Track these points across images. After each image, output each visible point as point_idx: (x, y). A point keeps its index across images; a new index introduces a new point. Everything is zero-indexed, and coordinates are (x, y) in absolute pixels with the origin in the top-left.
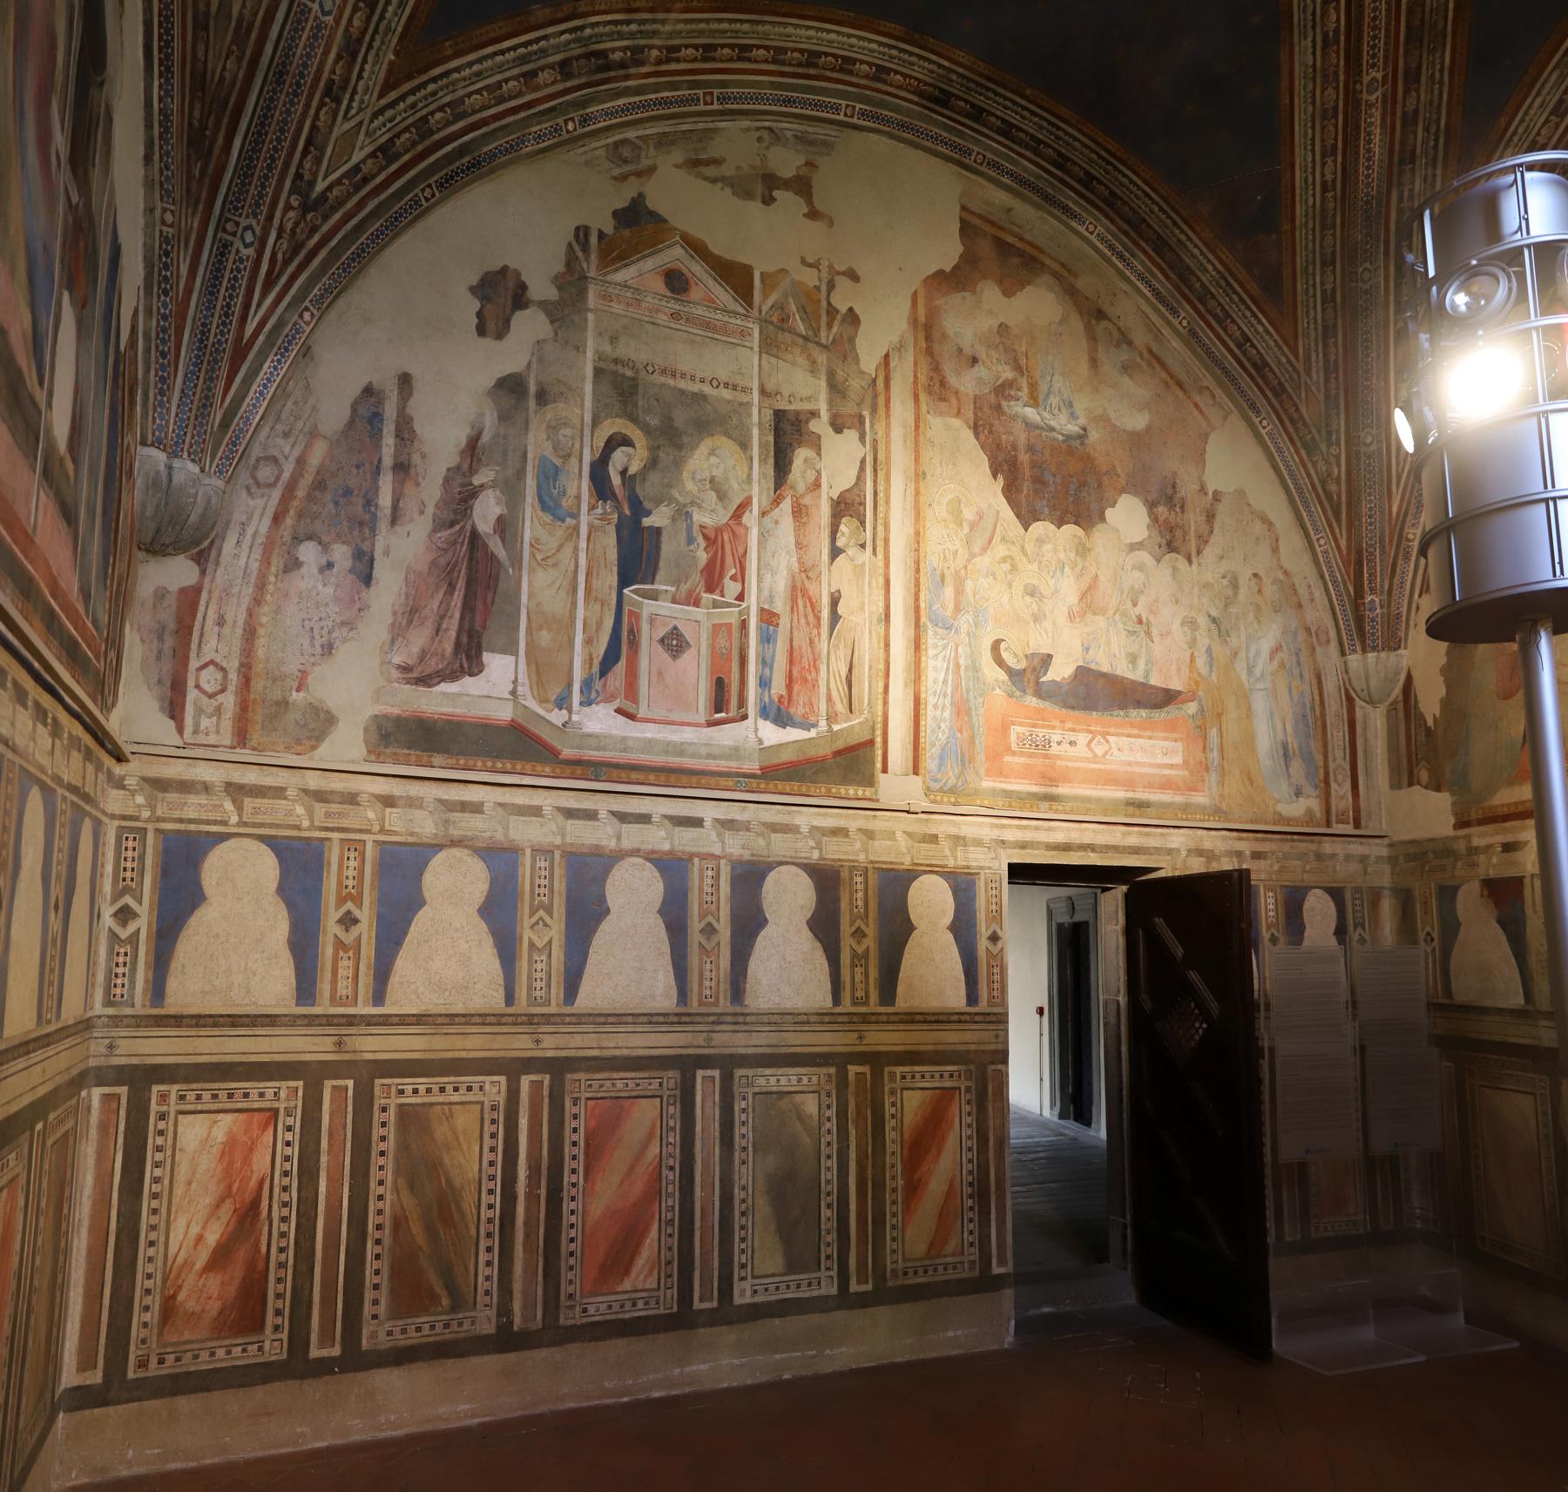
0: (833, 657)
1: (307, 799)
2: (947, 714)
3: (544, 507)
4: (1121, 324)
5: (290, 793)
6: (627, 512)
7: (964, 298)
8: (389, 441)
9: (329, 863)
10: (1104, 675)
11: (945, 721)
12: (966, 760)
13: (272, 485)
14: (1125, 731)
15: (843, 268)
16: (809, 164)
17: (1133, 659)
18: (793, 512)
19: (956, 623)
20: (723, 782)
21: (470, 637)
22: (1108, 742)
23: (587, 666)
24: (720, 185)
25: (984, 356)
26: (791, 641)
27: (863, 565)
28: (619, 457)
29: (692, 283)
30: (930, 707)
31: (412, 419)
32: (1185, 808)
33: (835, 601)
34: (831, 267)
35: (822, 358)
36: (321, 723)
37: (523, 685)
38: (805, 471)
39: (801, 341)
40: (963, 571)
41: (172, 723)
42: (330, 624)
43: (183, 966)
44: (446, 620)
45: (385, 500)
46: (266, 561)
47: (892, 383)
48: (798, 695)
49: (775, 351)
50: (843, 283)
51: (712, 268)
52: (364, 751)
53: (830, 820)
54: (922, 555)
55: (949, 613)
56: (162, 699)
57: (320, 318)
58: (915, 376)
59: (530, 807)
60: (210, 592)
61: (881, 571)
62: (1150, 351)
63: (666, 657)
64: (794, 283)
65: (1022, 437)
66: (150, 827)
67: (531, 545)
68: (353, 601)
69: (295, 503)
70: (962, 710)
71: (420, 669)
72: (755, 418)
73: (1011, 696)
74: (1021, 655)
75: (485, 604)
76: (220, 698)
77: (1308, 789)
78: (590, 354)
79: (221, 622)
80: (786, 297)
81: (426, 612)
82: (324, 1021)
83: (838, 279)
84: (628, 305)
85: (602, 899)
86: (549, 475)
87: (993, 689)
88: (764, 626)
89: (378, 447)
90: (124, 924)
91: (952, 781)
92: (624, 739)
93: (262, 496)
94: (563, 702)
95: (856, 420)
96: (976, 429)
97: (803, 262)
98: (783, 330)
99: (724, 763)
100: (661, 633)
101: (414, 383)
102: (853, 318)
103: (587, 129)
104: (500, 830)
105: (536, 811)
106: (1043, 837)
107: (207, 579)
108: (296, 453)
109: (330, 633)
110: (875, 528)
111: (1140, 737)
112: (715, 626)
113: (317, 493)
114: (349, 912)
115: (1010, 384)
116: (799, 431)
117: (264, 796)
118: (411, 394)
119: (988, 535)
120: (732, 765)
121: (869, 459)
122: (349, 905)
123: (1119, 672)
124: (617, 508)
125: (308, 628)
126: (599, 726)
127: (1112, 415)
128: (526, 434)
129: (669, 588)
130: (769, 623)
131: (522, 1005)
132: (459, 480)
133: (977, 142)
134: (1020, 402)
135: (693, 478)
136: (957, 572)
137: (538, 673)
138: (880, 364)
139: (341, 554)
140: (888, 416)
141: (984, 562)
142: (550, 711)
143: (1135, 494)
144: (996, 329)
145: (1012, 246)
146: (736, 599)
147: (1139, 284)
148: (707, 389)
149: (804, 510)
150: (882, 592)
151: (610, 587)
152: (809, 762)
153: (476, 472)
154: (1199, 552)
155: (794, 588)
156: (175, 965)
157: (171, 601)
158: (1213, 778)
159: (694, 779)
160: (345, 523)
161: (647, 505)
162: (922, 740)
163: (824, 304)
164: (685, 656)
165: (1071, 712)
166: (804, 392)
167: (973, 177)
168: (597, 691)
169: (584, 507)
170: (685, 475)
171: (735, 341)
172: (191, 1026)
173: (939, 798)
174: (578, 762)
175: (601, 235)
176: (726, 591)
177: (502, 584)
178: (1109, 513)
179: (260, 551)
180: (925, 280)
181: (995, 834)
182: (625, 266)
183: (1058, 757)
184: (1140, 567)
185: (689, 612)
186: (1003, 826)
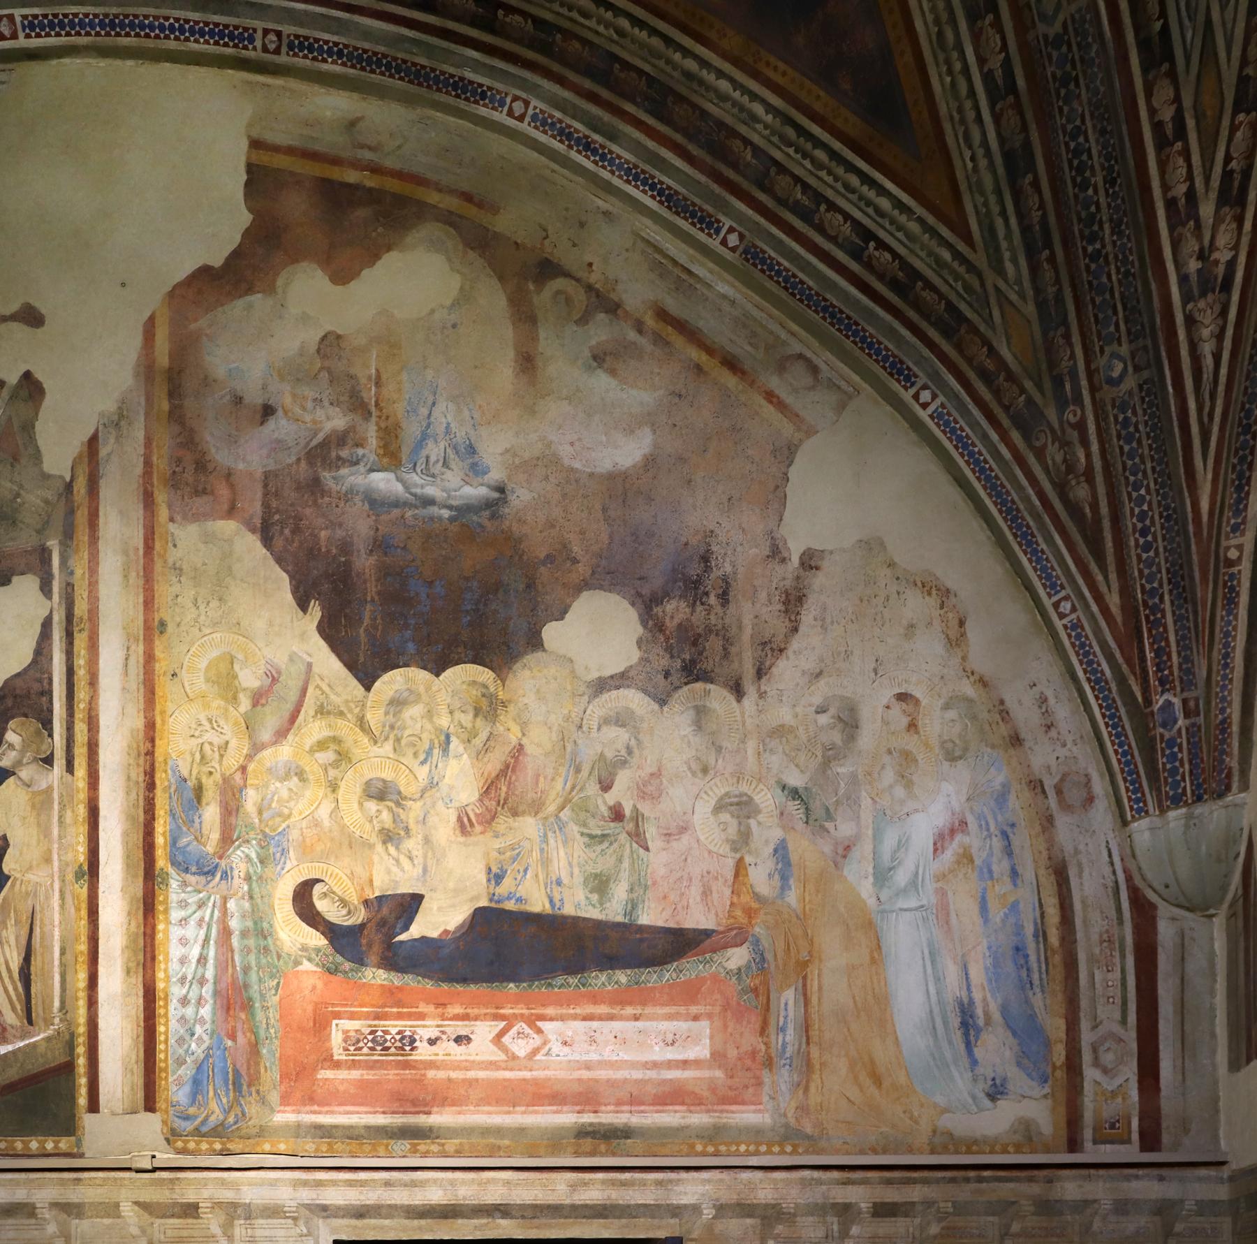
2: (206, 1011)
4: (594, 278)
7: (250, 307)
11: (202, 1021)
14: (578, 1011)
17: (600, 885)
19: (223, 863)
22: (539, 1031)
25: (288, 400)
27: (49, 789)
30: (174, 1004)
32: (714, 1135)
40: (238, 777)
47: (102, 483)
54: (159, 757)
55: (210, 848)
58: (148, 463)
61: (83, 796)
62: (662, 315)
65: (360, 526)
73: (332, 971)
74: (355, 900)
77: (1019, 1081)
87: (297, 963)
91: (216, 1116)
106: (400, 1197)
111: (611, 1018)
115: (341, 439)
119: (289, 707)
123: (569, 910)
127: (565, 451)
134: (361, 468)
136: (226, 780)
138: (80, 456)
140: (94, 539)
141: (284, 752)
144: (313, 348)
147: (630, 189)
150: (83, 829)
154: (760, 673)
158: (784, 1078)
165: (459, 988)
167: (278, 82)
173: (192, 1145)
178: (551, 633)
181: (306, 1195)
183: (432, 1065)
186: (319, 1184)
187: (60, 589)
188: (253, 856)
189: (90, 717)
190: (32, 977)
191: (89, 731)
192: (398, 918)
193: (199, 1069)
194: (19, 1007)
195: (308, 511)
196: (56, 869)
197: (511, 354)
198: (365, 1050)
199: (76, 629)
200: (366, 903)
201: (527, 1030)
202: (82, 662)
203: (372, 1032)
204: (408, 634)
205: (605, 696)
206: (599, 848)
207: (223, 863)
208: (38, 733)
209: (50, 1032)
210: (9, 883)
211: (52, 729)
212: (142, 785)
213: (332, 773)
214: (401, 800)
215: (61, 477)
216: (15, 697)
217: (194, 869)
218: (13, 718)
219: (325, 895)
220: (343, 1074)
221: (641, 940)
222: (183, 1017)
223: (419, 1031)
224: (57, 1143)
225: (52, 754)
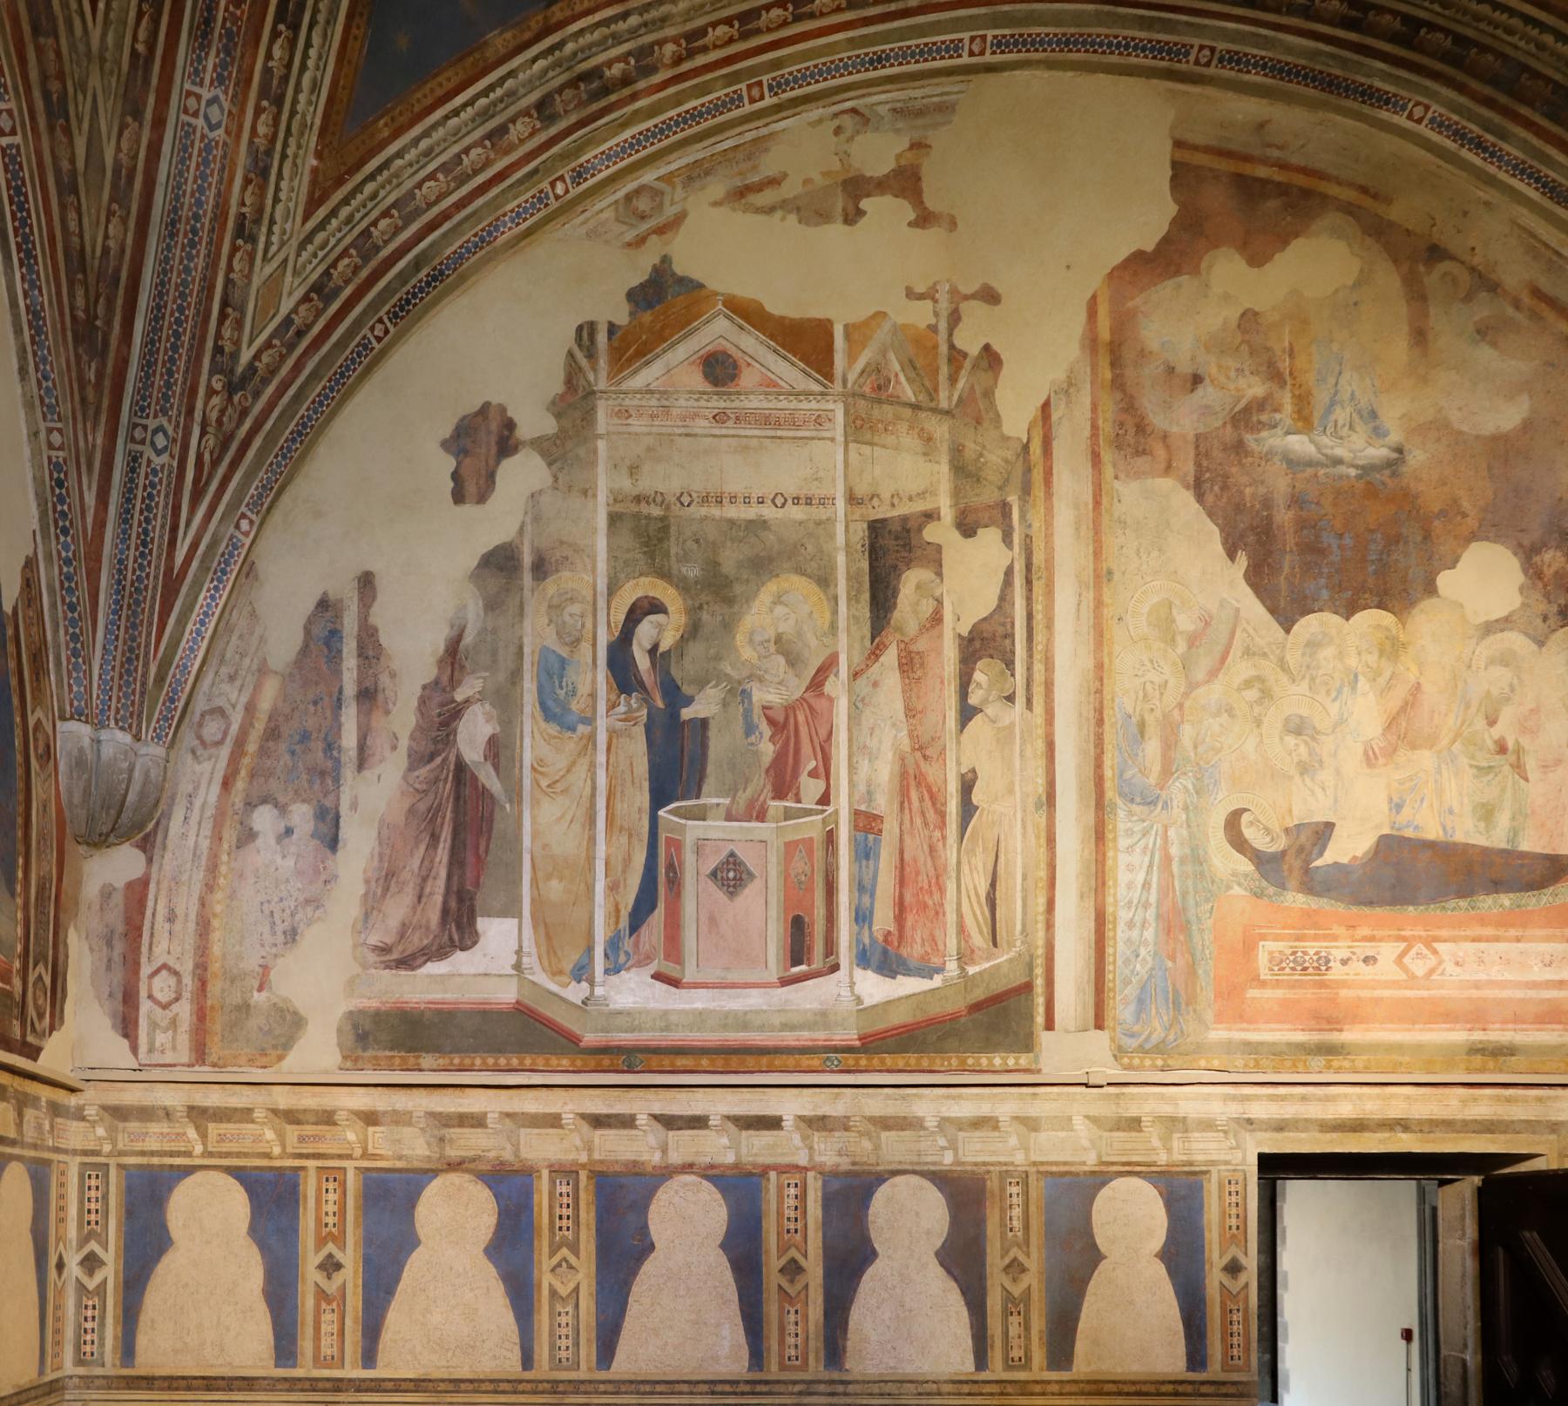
0: (965, 868)
1: (277, 1120)
2: (1149, 934)
3: (548, 715)
5: (259, 1114)
6: (660, 704)
8: (350, 663)
9: (305, 1197)
10: (1431, 845)
11: (1146, 943)
12: (1180, 1001)
13: (220, 743)
14: (1468, 933)
16: (917, 146)
17: (1487, 813)
18: (901, 665)
19: (1164, 794)
20: (806, 1061)
21: (461, 900)
22: (1435, 952)
23: (613, 920)
24: (779, 214)
25: (1214, 370)
26: (902, 852)
27: (1012, 724)
28: (646, 631)
29: (743, 365)
30: (1121, 926)
31: (377, 630)
33: (967, 786)
34: (954, 291)
35: (940, 430)
36: (289, 1025)
37: (529, 955)
38: (917, 604)
39: (908, 412)
40: (1176, 713)
41: (125, 1043)
42: (293, 904)
43: (153, 1321)
44: (430, 882)
45: (349, 739)
46: (218, 838)
47: (1055, 444)
48: (914, 929)
49: (868, 436)
50: (974, 312)
51: (772, 337)
52: (339, 1058)
53: (966, 1105)
55: (1152, 780)
56: (114, 1015)
57: (262, 524)
58: (1094, 427)
59: (545, 1116)
60: (158, 883)
61: (1041, 731)
63: (720, 895)
64: (896, 329)
65: (1280, 484)
66: (112, 1162)
68: (317, 872)
69: (246, 761)
70: (1174, 924)
71: (400, 948)
73: (1258, 895)
74: (1276, 828)
75: (478, 856)
76: (175, 1008)
78: (602, 497)
79: (171, 918)
80: (884, 353)
81: (405, 875)
82: (307, 1385)
83: (964, 306)
84: (652, 417)
85: (644, 1230)
86: (554, 671)
87: (1229, 888)
88: (860, 835)
89: (337, 672)
90: (91, 1273)
92: (666, 1013)
93: (210, 758)
94: (582, 972)
95: (997, 514)
96: (1198, 489)
97: (911, 294)
98: (880, 402)
99: (806, 1034)
100: (711, 864)
101: (378, 582)
102: (991, 359)
103: (585, 186)
104: (509, 1146)
105: (554, 1121)
107: (155, 869)
108: (244, 699)
109: (292, 915)
110: (1029, 669)
111: (1497, 939)
112: (787, 845)
113: (271, 744)
114: (330, 1256)
115: (1261, 405)
116: (908, 546)
117: (229, 1121)
118: (374, 598)
120: (820, 1036)
121: (1019, 568)
122: (331, 1247)
123: (1459, 837)
125: (267, 912)
126: (631, 999)
127: (1454, 417)
128: (521, 622)
129: (721, 801)
130: (868, 830)
131: (542, 1368)
132: (437, 699)
133: (1199, 30)
134: (1279, 431)
135: (751, 641)
137: (548, 937)
139: (302, 815)
140: (1049, 495)
141: (1213, 693)
142: (566, 986)
143: (1497, 539)
145: (1264, 182)
148: (768, 512)
149: (917, 659)
150: (1042, 762)
151: (640, 810)
152: (932, 1023)
153: (459, 683)
155: (904, 774)
156: (144, 1319)
157: (118, 899)
159: (764, 1060)
160: (304, 776)
161: (687, 690)
162: (1109, 976)
163: (944, 349)
164: (746, 891)
165: (1366, 910)
166: (914, 487)
168: (627, 953)
169: (602, 707)
172: (162, 1389)
173: (1136, 1062)
174: (605, 1050)
178: (1444, 580)
179: (210, 826)
180: (1110, 275)
182: (648, 363)
183: (1344, 984)
184: (1505, 659)
185: (748, 829)
188: (1190, 787)
192: (1314, 845)
193: (1143, 988)
195: (1234, 470)
197: (1405, 328)
198: (1287, 970)
199: (1034, 577)
200: (1287, 831)
201: (1425, 951)
202: (1040, 607)
203: (1294, 953)
204: (1323, 581)
205: (1491, 638)
206: (1485, 779)
207: (1164, 794)
209: (1012, 954)
212: (1093, 722)
213: (1257, 710)
214: (1315, 734)
217: (1138, 800)
219: (1252, 823)
220: (1268, 993)
221: (1522, 866)
222: (1129, 940)
223: (1333, 951)
224: (1017, 1059)
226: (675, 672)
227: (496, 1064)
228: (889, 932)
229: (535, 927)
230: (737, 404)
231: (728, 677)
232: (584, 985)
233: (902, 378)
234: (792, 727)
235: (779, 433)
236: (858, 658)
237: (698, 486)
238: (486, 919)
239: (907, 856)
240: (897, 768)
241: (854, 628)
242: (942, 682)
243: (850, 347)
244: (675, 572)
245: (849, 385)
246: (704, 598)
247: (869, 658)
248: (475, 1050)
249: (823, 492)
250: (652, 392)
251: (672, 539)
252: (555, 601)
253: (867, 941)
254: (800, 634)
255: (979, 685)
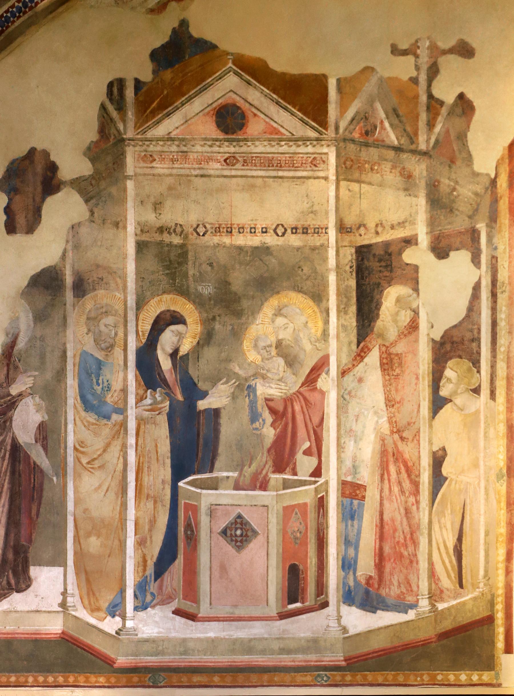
0: (436, 527)
6: (180, 397)
15: (451, 43)
18: (382, 364)
21: (16, 552)
23: (141, 569)
26: (381, 514)
27: (477, 412)
29: (250, 115)
34: (433, 47)
37: (73, 595)
38: (397, 314)
39: (391, 154)
48: (391, 574)
49: (356, 175)
63: (229, 549)
67: (75, 448)
72: (332, 262)
75: (30, 518)
78: (131, 228)
80: (371, 102)
83: (442, 61)
84: (173, 161)
88: (347, 501)
92: (184, 640)
95: (467, 239)
97: (395, 51)
98: (367, 145)
110: (493, 367)
112: (285, 509)
116: (389, 267)
120: (312, 658)
121: (486, 283)
124: (167, 394)
126: (156, 630)
128: (65, 331)
129: (230, 474)
130: (353, 496)
135: (256, 346)
137: (88, 581)
138: (502, 158)
142: (102, 619)
146: (312, 475)
148: (270, 240)
149: (396, 360)
151: (163, 482)
152: (407, 647)
153: (14, 380)
155: (384, 453)
159: (266, 677)
161: (202, 386)
163: (424, 98)
164: (251, 545)
166: (395, 217)
168: (152, 594)
169: (132, 400)
170: (247, 345)
171: (305, 174)
174: (134, 670)
175: (138, 84)
176: (298, 468)
177: (47, 494)
182: (168, 115)
185: (252, 496)
187: (487, 260)
189: (508, 358)
190: (463, 553)
191: (508, 367)
194: (453, 575)
196: (482, 472)
199: (499, 291)
202: (503, 316)
208: (469, 370)
209: (476, 594)
210: (447, 483)
211: (479, 367)
215: (488, 175)
216: (453, 343)
218: (451, 358)
224: (480, 676)
225: (480, 386)
226: (192, 372)
227: (45, 681)
228: (371, 577)
229: (77, 574)
230: (244, 149)
231: (237, 376)
232: (118, 619)
233: (387, 124)
234: (290, 415)
235: (281, 174)
236: (345, 360)
237: (211, 219)
238: (38, 568)
239: (386, 517)
240: (378, 447)
241: (342, 335)
242: (417, 378)
243: (342, 99)
244: (192, 290)
245: (341, 131)
246: (216, 311)
247: (355, 359)
248: (28, 671)
249: (317, 223)
250: (172, 140)
251: (190, 263)
252: (93, 315)
253: (351, 583)
254: (297, 340)
255: (449, 380)
